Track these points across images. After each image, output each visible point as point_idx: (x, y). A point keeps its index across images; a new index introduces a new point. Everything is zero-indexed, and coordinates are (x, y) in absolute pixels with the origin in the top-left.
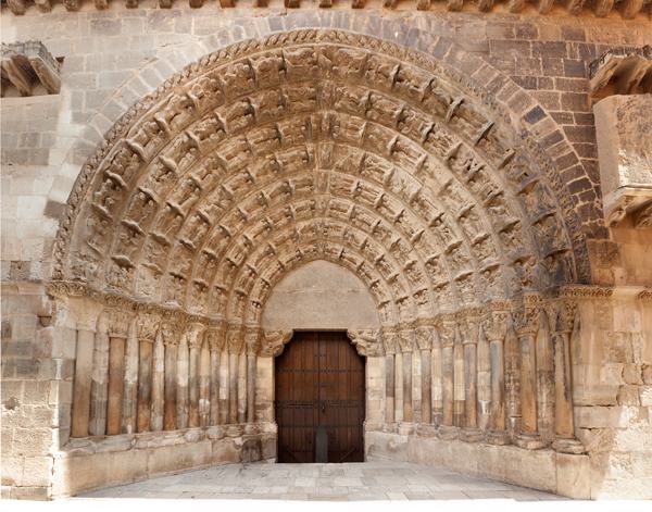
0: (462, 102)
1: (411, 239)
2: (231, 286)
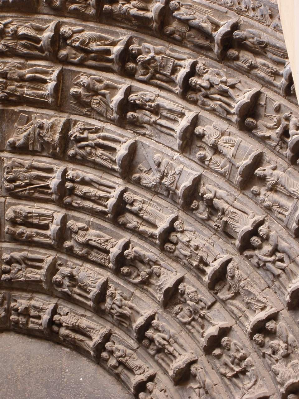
1: (206, 279)
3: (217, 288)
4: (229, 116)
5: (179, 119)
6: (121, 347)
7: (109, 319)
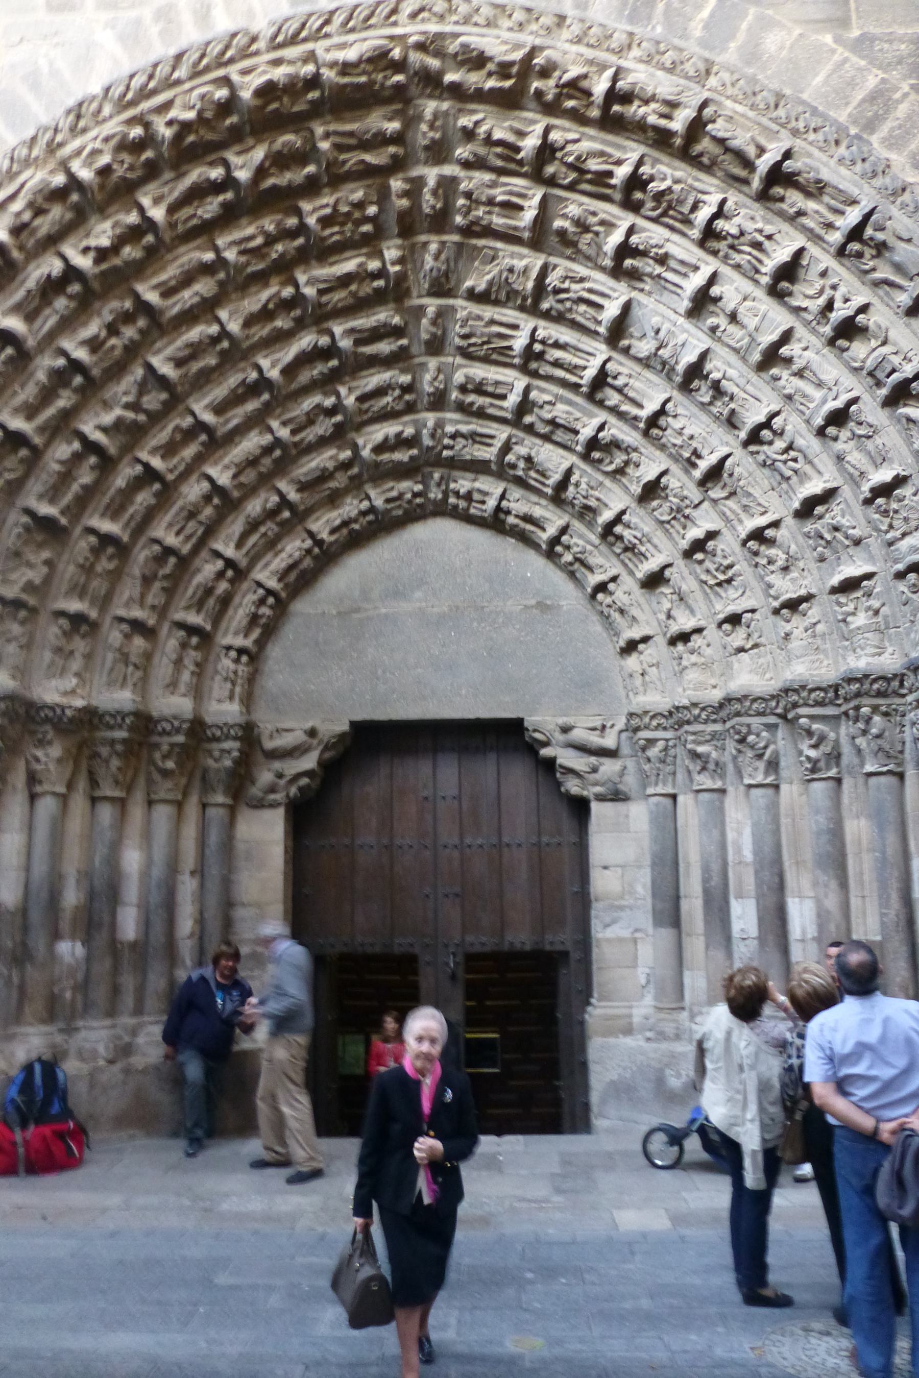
0: (787, 155)
1: (697, 474)
2: (162, 611)
3: (709, 485)
4: (757, 276)
5: (691, 275)
6: (581, 542)
7: (569, 509)
